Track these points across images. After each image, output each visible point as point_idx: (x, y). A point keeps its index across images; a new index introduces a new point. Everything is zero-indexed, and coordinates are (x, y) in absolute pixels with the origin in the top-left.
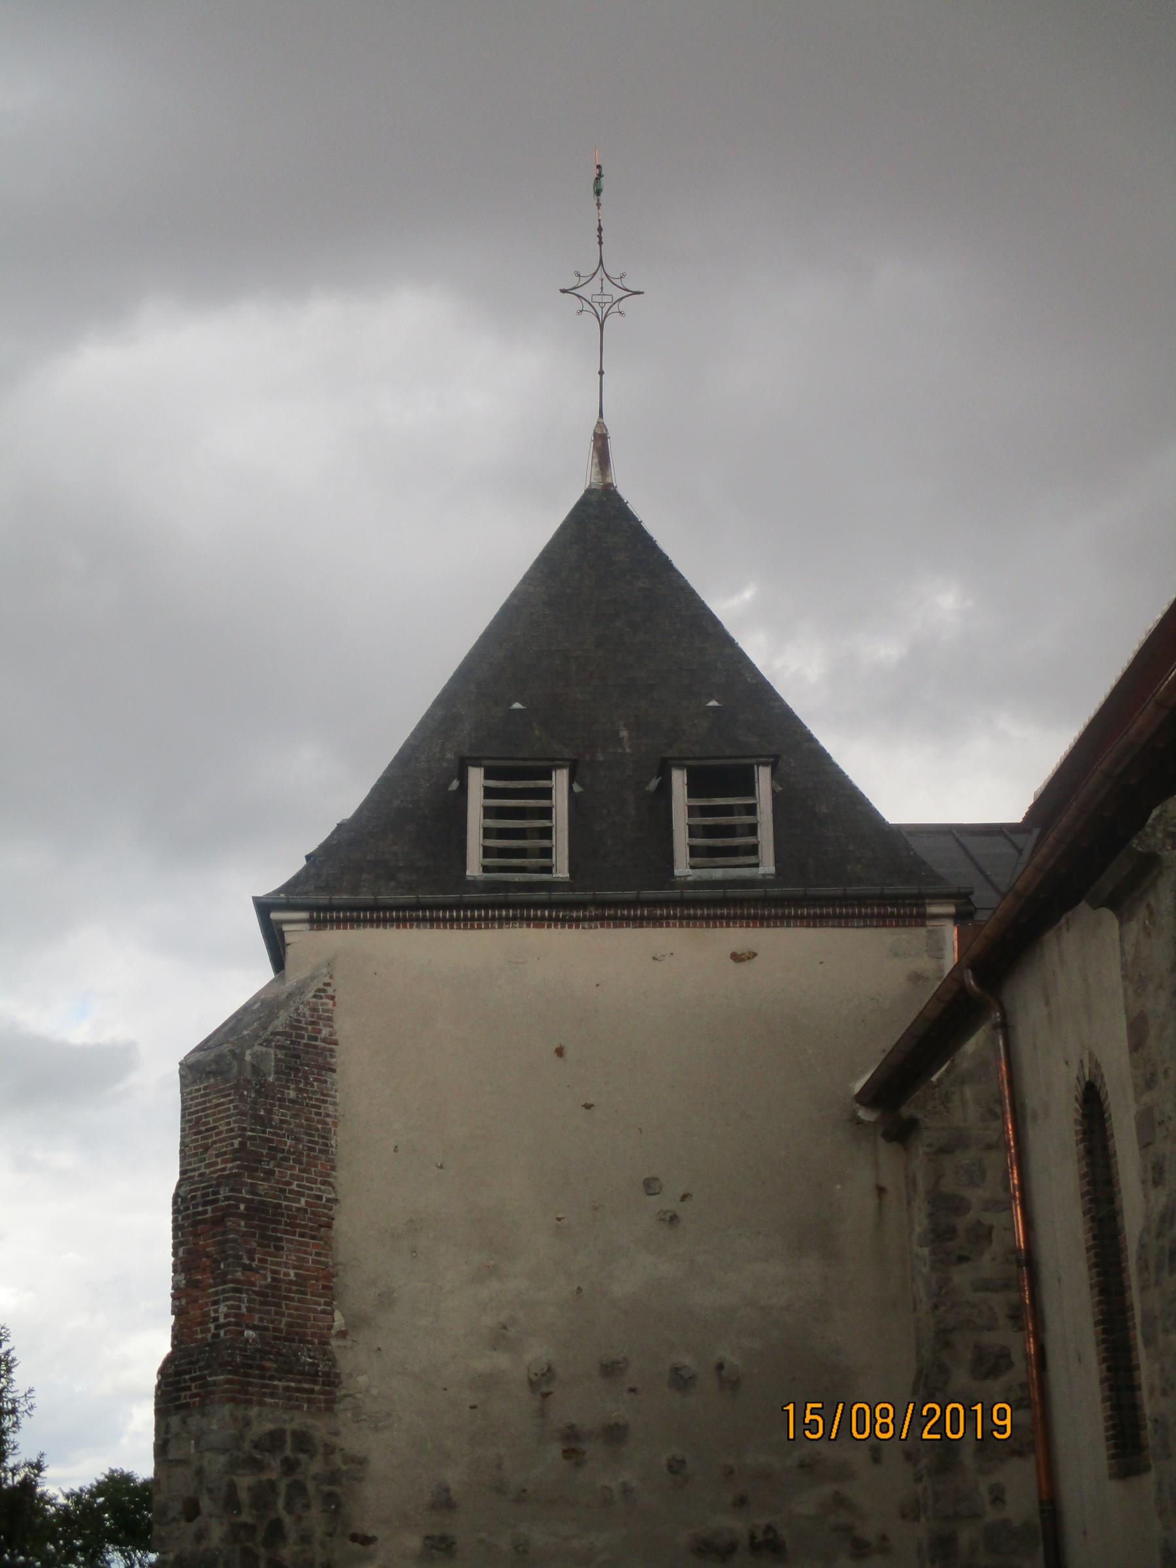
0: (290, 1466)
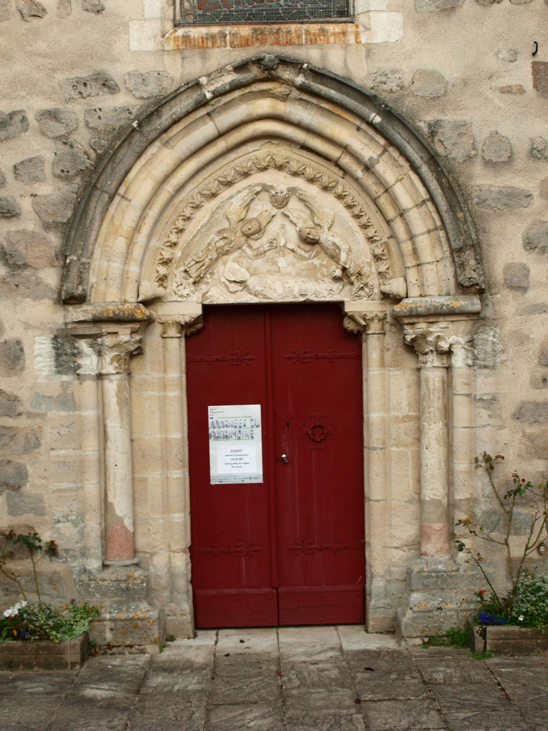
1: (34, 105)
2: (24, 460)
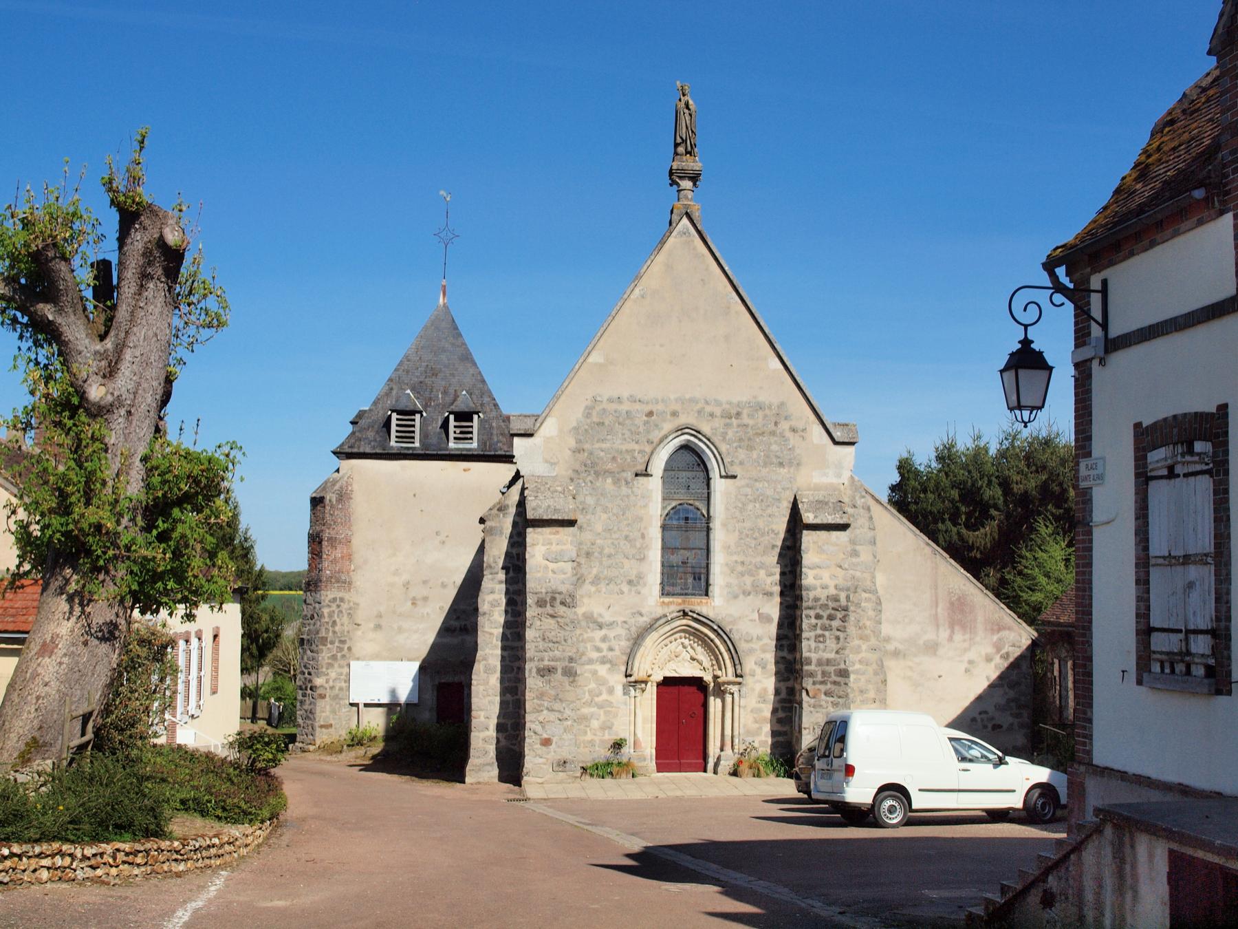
0: (338, 606)
1: (620, 619)
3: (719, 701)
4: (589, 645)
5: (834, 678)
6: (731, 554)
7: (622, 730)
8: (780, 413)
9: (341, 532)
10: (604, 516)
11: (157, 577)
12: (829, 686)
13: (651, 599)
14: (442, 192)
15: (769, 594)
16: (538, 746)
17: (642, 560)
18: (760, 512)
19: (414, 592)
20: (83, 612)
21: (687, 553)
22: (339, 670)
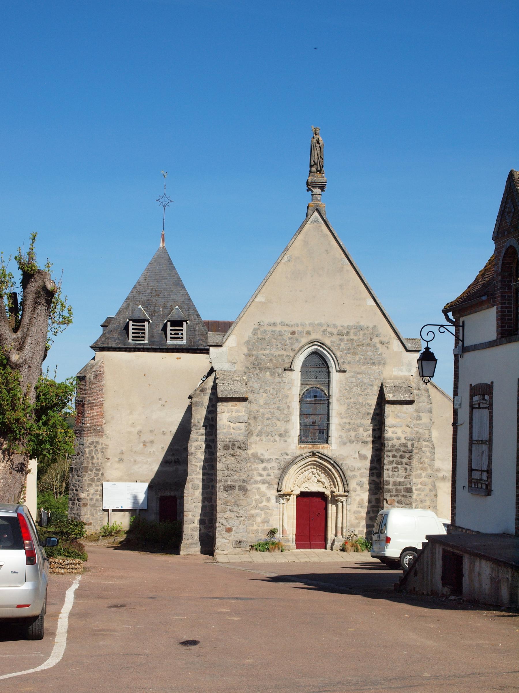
0: (95, 447)
2: (270, 517)
3: (334, 506)
4: (255, 473)
5: (403, 493)
6: (342, 418)
7: (275, 524)
8: (374, 332)
9: (96, 399)
10: (265, 395)
11: (42, 442)
12: (400, 498)
13: (293, 445)
14: (162, 172)
15: (365, 442)
16: (224, 532)
17: (287, 421)
18: (360, 393)
19: (143, 438)
20: (9, 459)
21: (316, 418)
22: (96, 488)
